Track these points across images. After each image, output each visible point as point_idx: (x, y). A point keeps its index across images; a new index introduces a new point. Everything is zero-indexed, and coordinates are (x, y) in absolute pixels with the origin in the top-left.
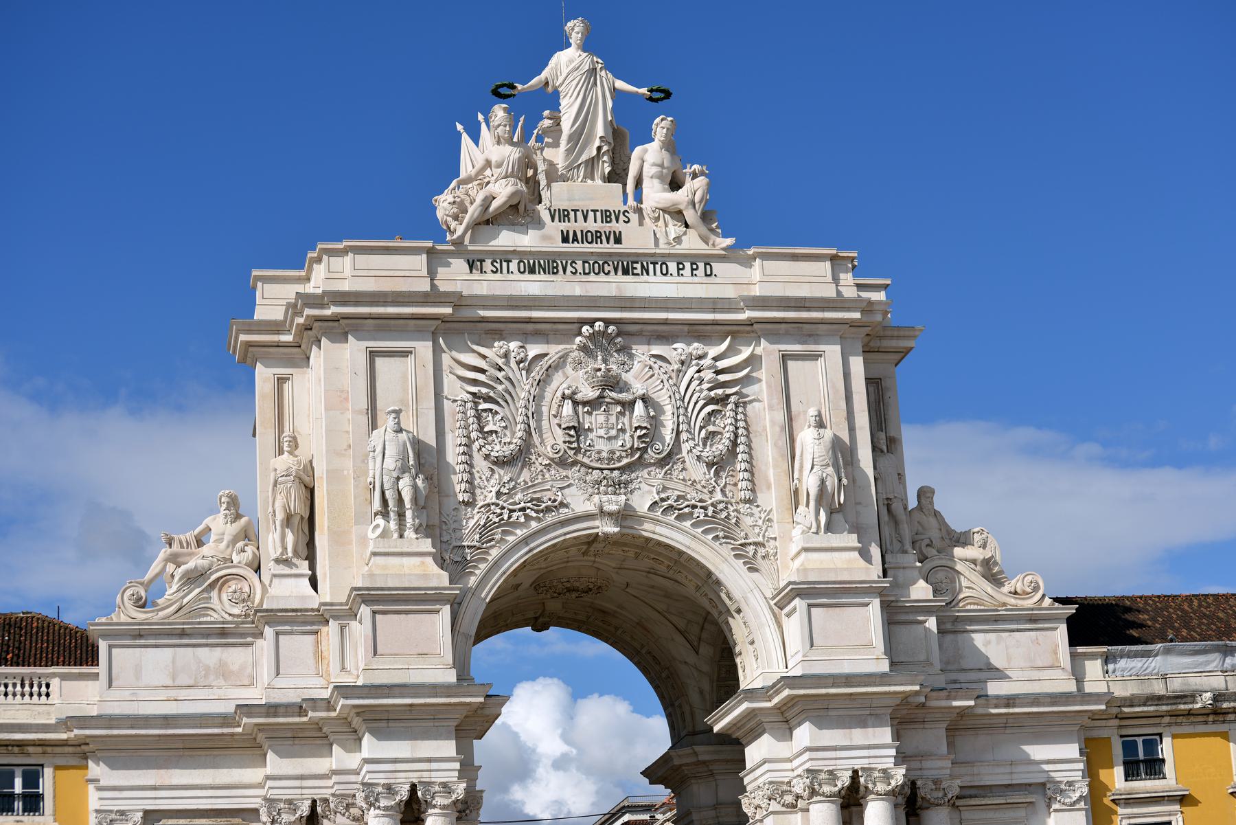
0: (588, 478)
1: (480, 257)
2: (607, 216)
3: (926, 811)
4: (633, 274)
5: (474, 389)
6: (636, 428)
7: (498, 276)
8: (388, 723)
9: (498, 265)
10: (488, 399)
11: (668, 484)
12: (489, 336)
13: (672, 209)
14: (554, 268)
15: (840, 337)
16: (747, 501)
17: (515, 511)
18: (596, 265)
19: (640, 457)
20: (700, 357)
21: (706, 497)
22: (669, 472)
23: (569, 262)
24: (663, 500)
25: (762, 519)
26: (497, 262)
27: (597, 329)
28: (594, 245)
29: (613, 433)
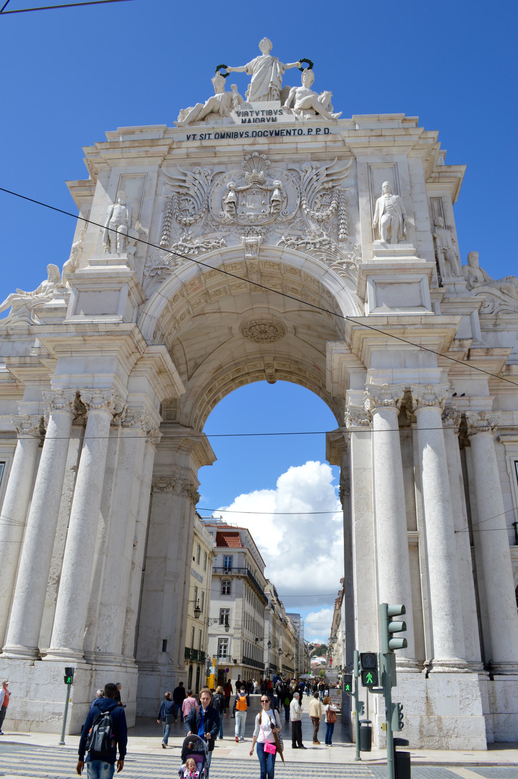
1: (194, 133)
2: (270, 112)
3: (474, 436)
5: (178, 191)
6: (273, 201)
8: (71, 353)
9: (204, 136)
12: (193, 167)
13: (308, 106)
14: (235, 135)
15: (408, 157)
17: (193, 248)
18: (260, 133)
19: (275, 220)
24: (287, 240)
27: (253, 155)
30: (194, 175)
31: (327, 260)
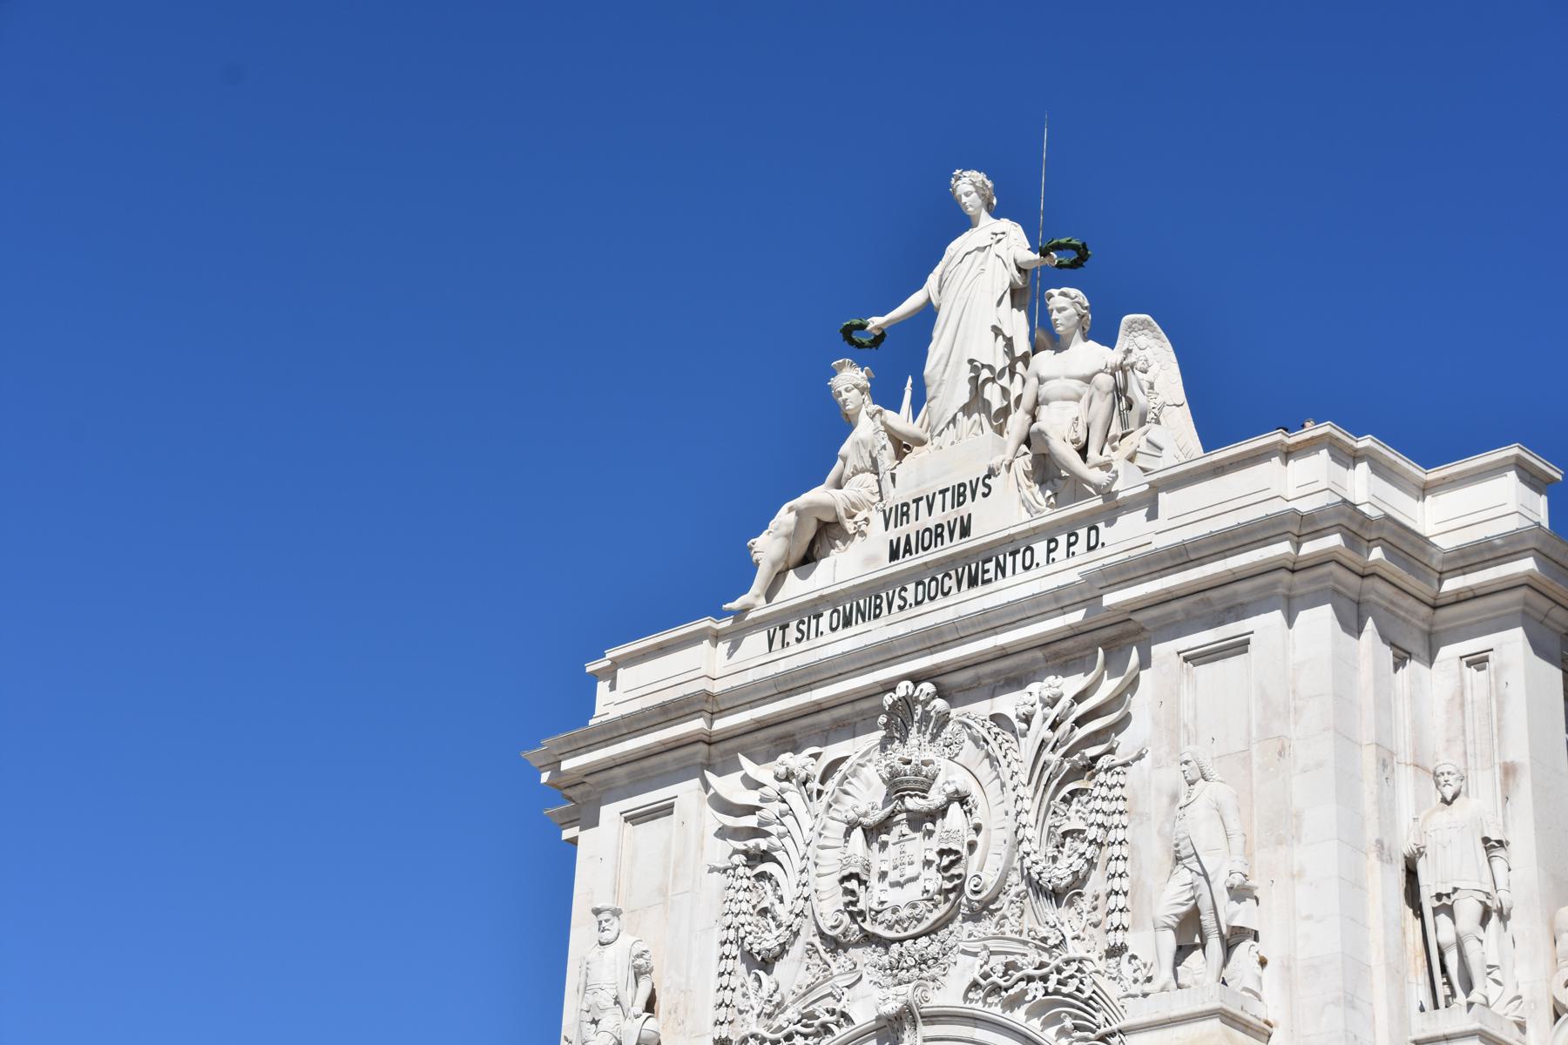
0: (885, 959)
2: (960, 494)
4: (985, 582)
6: (942, 853)
7: (804, 645)
10: (766, 856)
11: (993, 945)
16: (1115, 952)
18: (934, 583)
20: (1054, 702)
21: (1045, 958)
22: (1002, 921)
23: (898, 590)
25: (1141, 980)
26: (804, 623)
28: (932, 549)
29: (910, 872)
30: (777, 785)
31: (1077, 1028)
